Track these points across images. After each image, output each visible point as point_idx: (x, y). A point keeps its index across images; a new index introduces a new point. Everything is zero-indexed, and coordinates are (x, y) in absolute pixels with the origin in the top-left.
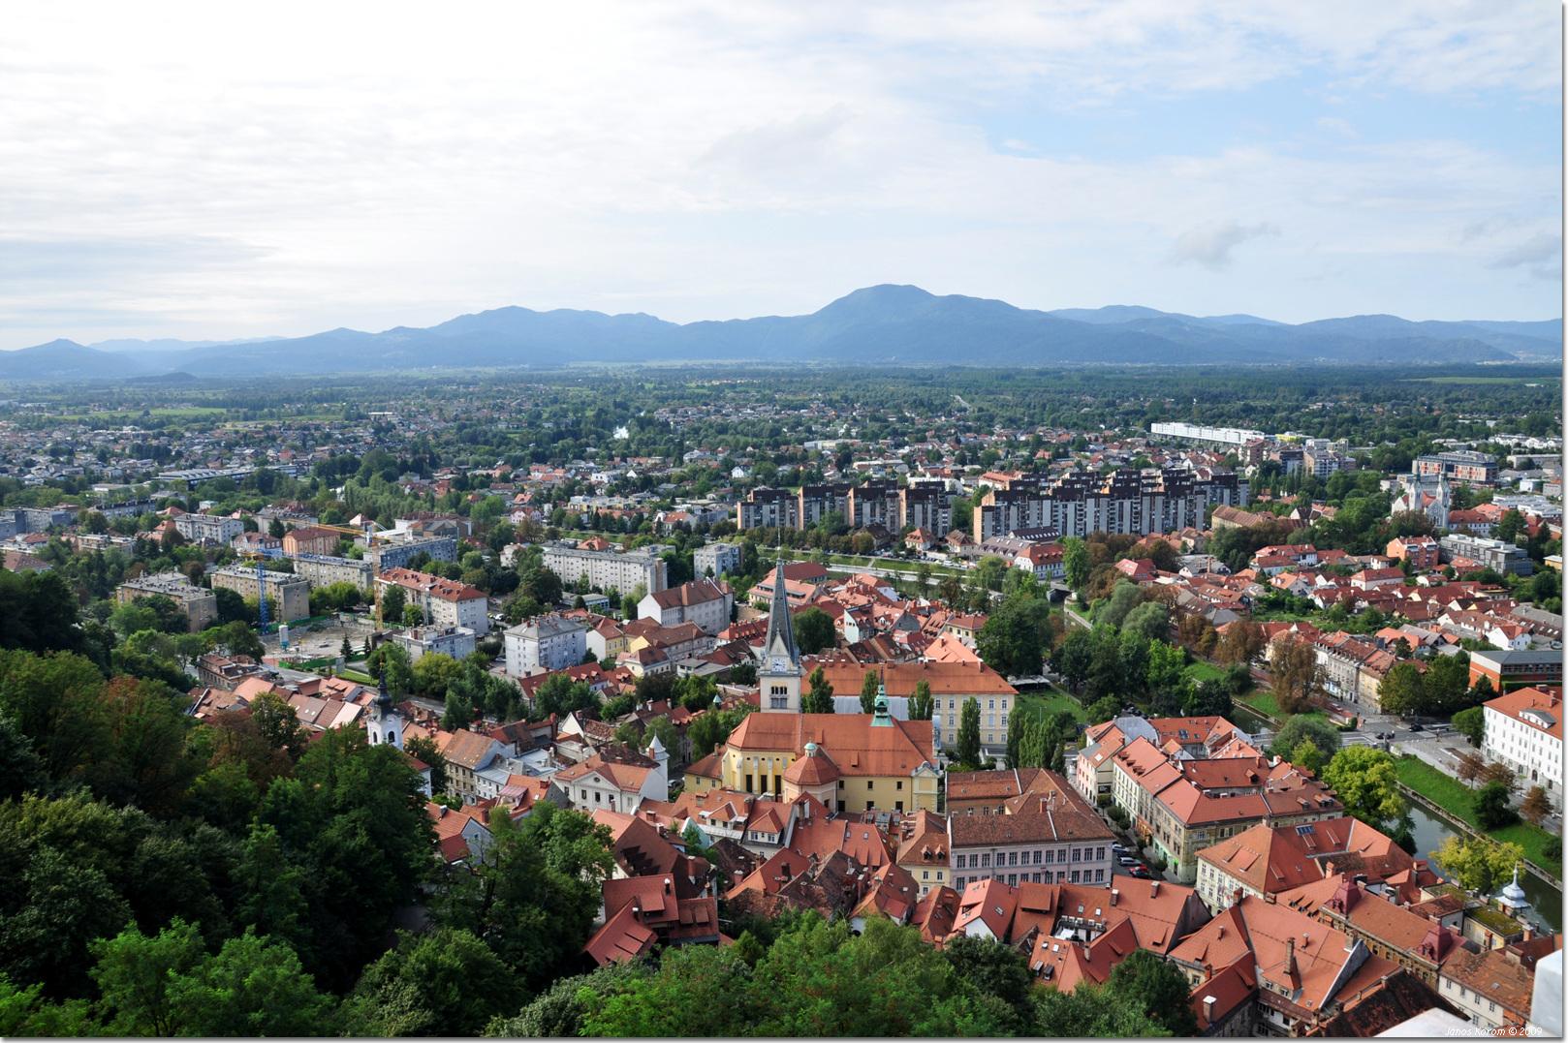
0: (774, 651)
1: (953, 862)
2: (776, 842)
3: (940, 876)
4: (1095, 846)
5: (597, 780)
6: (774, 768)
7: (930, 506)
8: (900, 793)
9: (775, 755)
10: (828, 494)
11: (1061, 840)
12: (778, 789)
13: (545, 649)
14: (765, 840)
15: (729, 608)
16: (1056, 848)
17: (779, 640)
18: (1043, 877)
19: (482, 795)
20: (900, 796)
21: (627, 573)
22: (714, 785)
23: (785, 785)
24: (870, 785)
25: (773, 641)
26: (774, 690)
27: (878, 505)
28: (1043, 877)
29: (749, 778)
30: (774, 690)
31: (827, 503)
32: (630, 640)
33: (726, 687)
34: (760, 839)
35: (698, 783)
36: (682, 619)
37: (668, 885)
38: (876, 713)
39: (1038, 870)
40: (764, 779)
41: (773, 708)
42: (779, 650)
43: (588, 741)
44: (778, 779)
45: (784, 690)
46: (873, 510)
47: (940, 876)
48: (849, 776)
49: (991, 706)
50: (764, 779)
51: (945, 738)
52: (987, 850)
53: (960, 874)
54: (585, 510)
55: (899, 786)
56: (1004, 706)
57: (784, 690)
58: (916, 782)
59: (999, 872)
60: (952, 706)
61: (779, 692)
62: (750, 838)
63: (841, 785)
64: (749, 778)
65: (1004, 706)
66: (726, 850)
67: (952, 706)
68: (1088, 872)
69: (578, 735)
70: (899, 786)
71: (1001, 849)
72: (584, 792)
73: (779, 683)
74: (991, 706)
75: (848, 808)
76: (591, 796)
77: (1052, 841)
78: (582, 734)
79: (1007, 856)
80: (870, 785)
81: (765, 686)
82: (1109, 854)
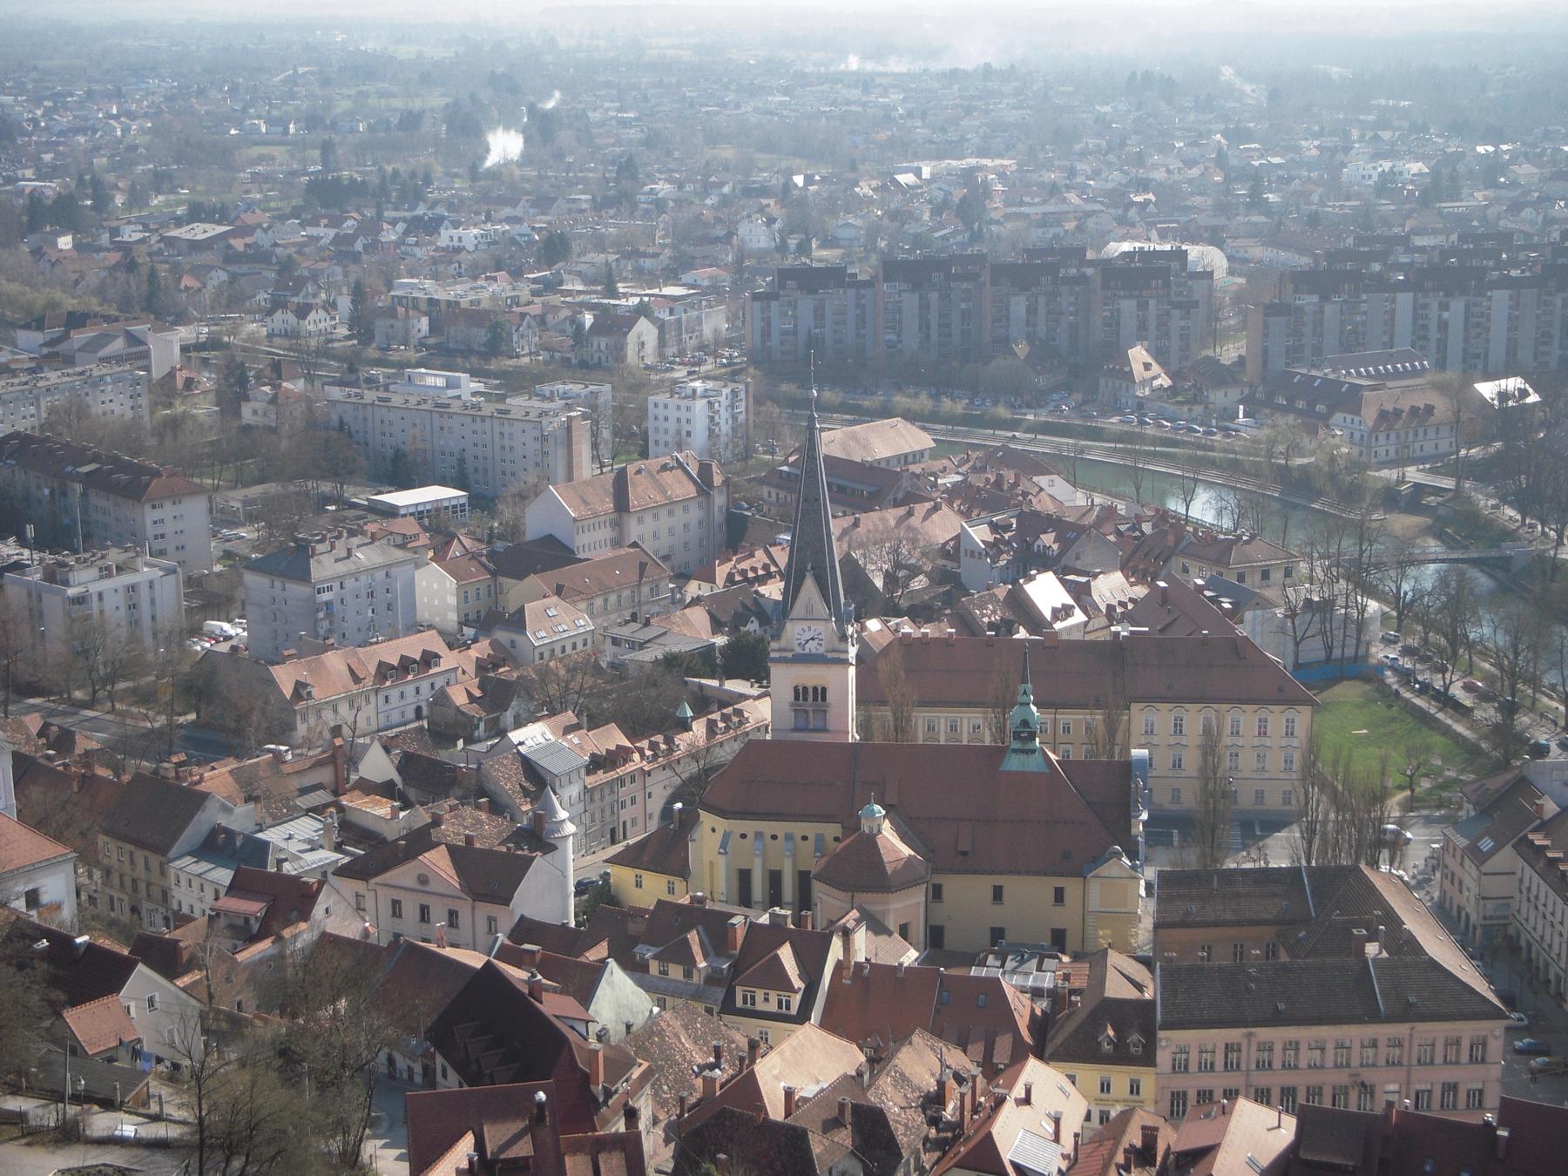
0: (798, 609)
1: (1163, 1057)
2: (794, 1011)
3: (1135, 1088)
4: (1467, 1030)
5: (423, 880)
6: (795, 856)
7: (1152, 303)
8: (1059, 909)
9: (798, 828)
10: (937, 276)
11: (1389, 1019)
12: (804, 901)
13: (328, 604)
14: (772, 1007)
15: (719, 517)
16: (1384, 1031)
17: (809, 584)
18: (1353, 1095)
19: (185, 910)
20: (1065, 917)
21: (507, 443)
22: (671, 891)
23: (819, 890)
24: (998, 893)
25: (797, 589)
26: (800, 693)
27: (1042, 301)
28: (1353, 1095)
29: (744, 877)
30: (800, 693)
31: (934, 297)
32: (507, 582)
33: (703, 681)
34: (760, 1006)
35: (639, 885)
36: (617, 543)
37: (540, 1105)
38: (1016, 745)
39: (1342, 1078)
40: (775, 878)
41: (796, 730)
42: (809, 608)
43: (412, 794)
44: (804, 880)
45: (821, 693)
46: (1032, 311)
47: (1135, 1088)
48: (951, 871)
49: (1262, 732)
50: (775, 878)
51: (1163, 798)
52: (1234, 1035)
53: (1179, 1083)
54: (424, 307)
55: (1059, 895)
56: (1290, 733)
57: (821, 693)
58: (1095, 888)
59: (1261, 1079)
60: (1179, 729)
61: (811, 700)
62: (739, 1003)
63: (937, 893)
64: (744, 877)
65: (1290, 733)
66: (685, 1027)
67: (1179, 729)
68: (1453, 1088)
69: (391, 783)
70: (1059, 895)
71: (1264, 1034)
72: (396, 904)
73: (811, 676)
74: (1262, 732)
75: (951, 940)
76: (410, 910)
77: (1374, 1017)
78: (398, 779)
79: (1278, 1048)
80: (998, 893)
81: (784, 678)
82: (1496, 1047)
